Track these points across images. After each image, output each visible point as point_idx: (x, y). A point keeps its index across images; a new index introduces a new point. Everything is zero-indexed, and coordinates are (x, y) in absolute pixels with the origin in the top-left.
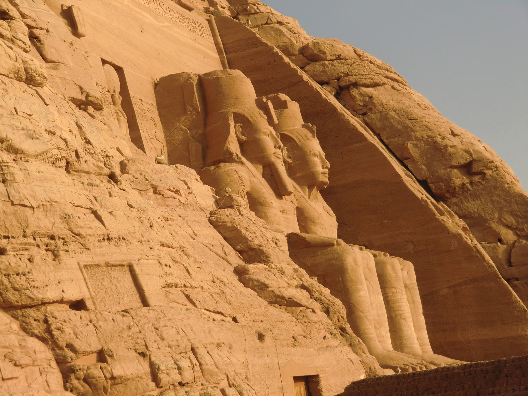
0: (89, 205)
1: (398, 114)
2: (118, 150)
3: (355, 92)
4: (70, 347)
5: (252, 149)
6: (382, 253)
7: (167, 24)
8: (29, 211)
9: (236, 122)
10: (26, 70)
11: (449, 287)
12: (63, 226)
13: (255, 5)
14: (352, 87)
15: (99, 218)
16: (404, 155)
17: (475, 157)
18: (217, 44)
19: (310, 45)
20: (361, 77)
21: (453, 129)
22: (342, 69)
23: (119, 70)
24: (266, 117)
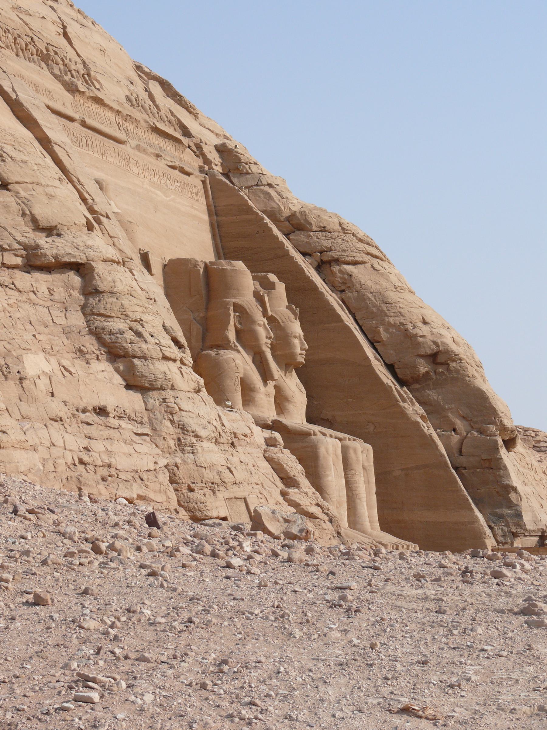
0: (226, 464)
1: (375, 296)
3: (336, 268)
5: (247, 338)
7: (173, 196)
8: (203, 469)
9: (235, 311)
11: (402, 470)
12: (218, 477)
13: (247, 164)
14: (334, 263)
15: (231, 472)
16: (375, 338)
17: (441, 348)
18: (208, 206)
19: (298, 214)
20: (344, 254)
21: (425, 317)
22: (327, 243)
24: (260, 308)
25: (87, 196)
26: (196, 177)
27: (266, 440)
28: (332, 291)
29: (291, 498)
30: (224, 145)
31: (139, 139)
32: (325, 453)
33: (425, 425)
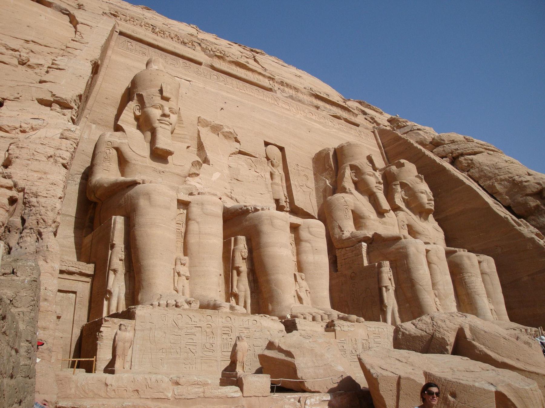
3: (461, 159)
6: (462, 249)
7: (335, 130)
9: (351, 170)
11: (528, 276)
18: (378, 144)
23: (282, 149)
30: (392, 117)
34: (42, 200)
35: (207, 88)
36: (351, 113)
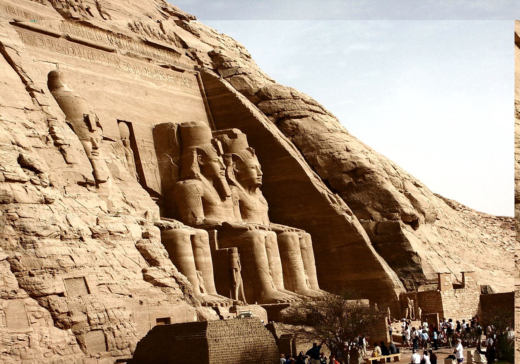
2: (100, 207)
3: (288, 122)
4: (57, 311)
7: (165, 85)
10: (45, 199)
13: (228, 62)
18: (201, 90)
20: (292, 112)
22: (281, 106)
23: (129, 125)
25: (27, 79)
26: (190, 72)
27: (143, 234)
28: (287, 137)
29: (148, 274)
30: (213, 52)
31: (132, 49)
32: (258, 240)
33: (350, 217)
34: (185, 281)
35: (69, 68)
36: (176, 54)
